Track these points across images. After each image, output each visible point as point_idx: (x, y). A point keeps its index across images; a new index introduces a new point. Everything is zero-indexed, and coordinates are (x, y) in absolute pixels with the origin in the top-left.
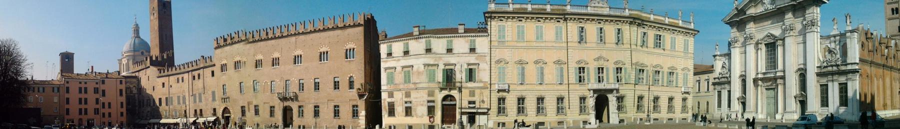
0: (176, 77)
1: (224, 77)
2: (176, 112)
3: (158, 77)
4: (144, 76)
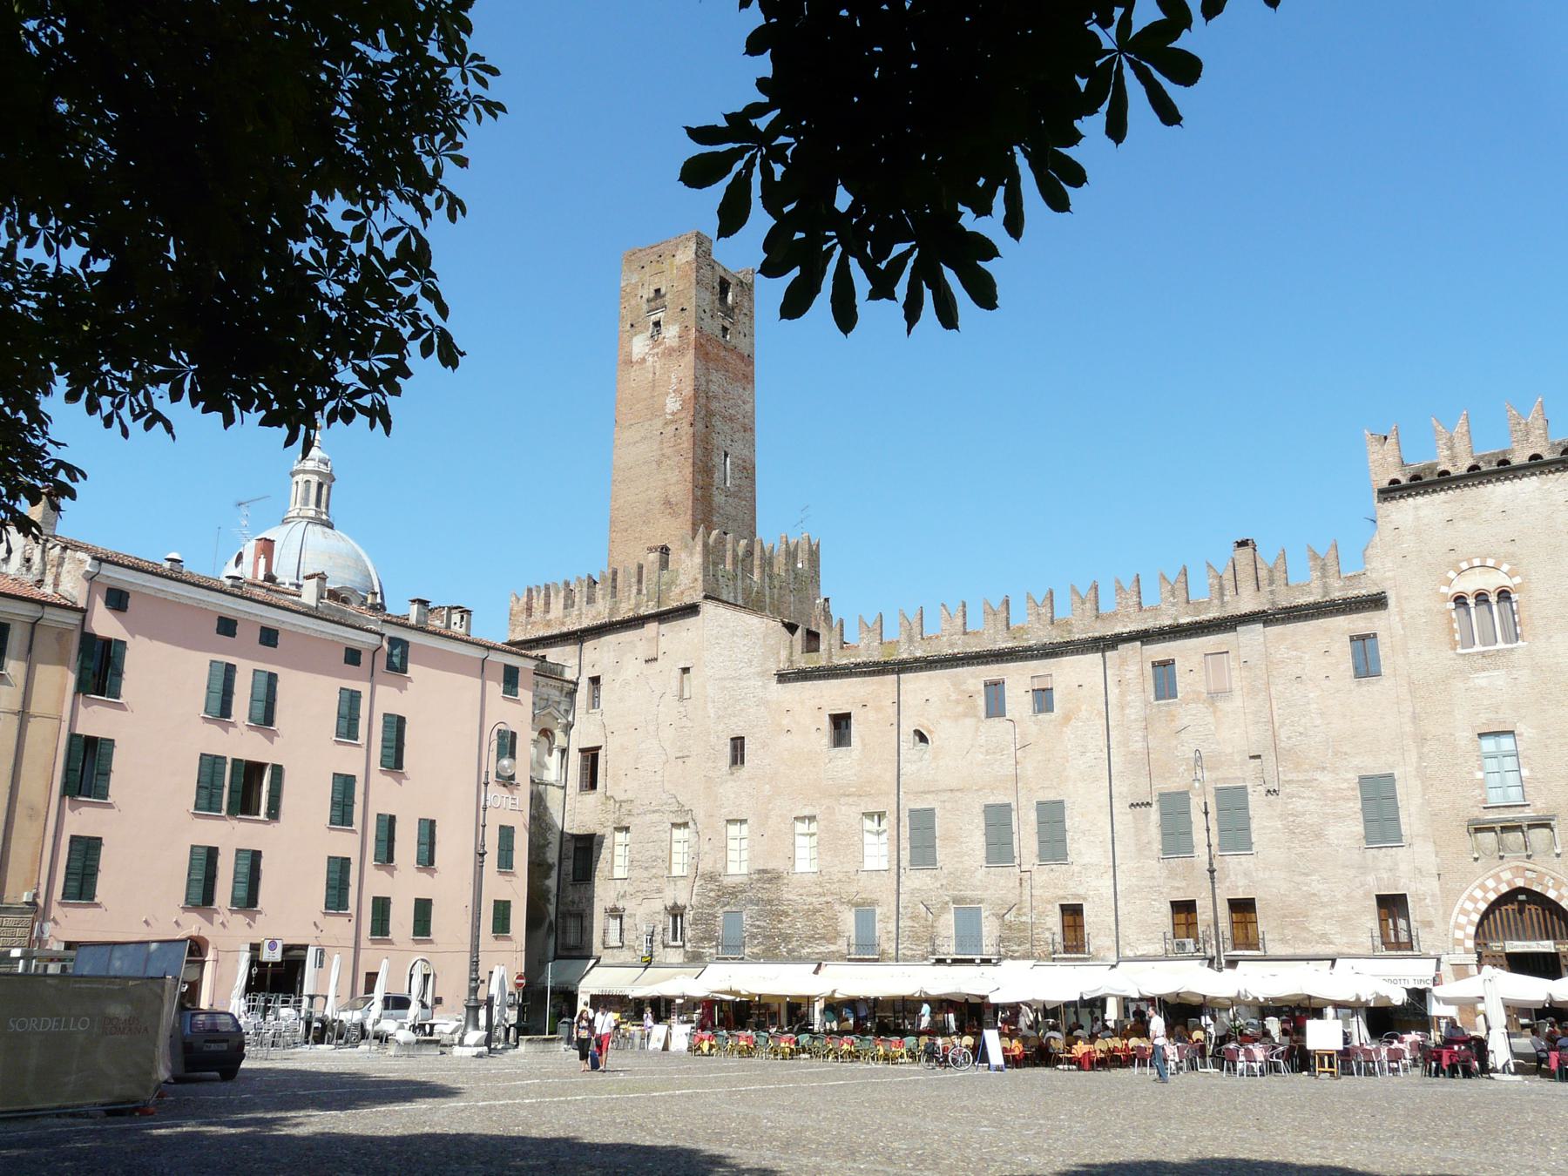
0: (974, 678)
1: (1492, 680)
2: (968, 918)
3: (783, 678)
4: (633, 667)
